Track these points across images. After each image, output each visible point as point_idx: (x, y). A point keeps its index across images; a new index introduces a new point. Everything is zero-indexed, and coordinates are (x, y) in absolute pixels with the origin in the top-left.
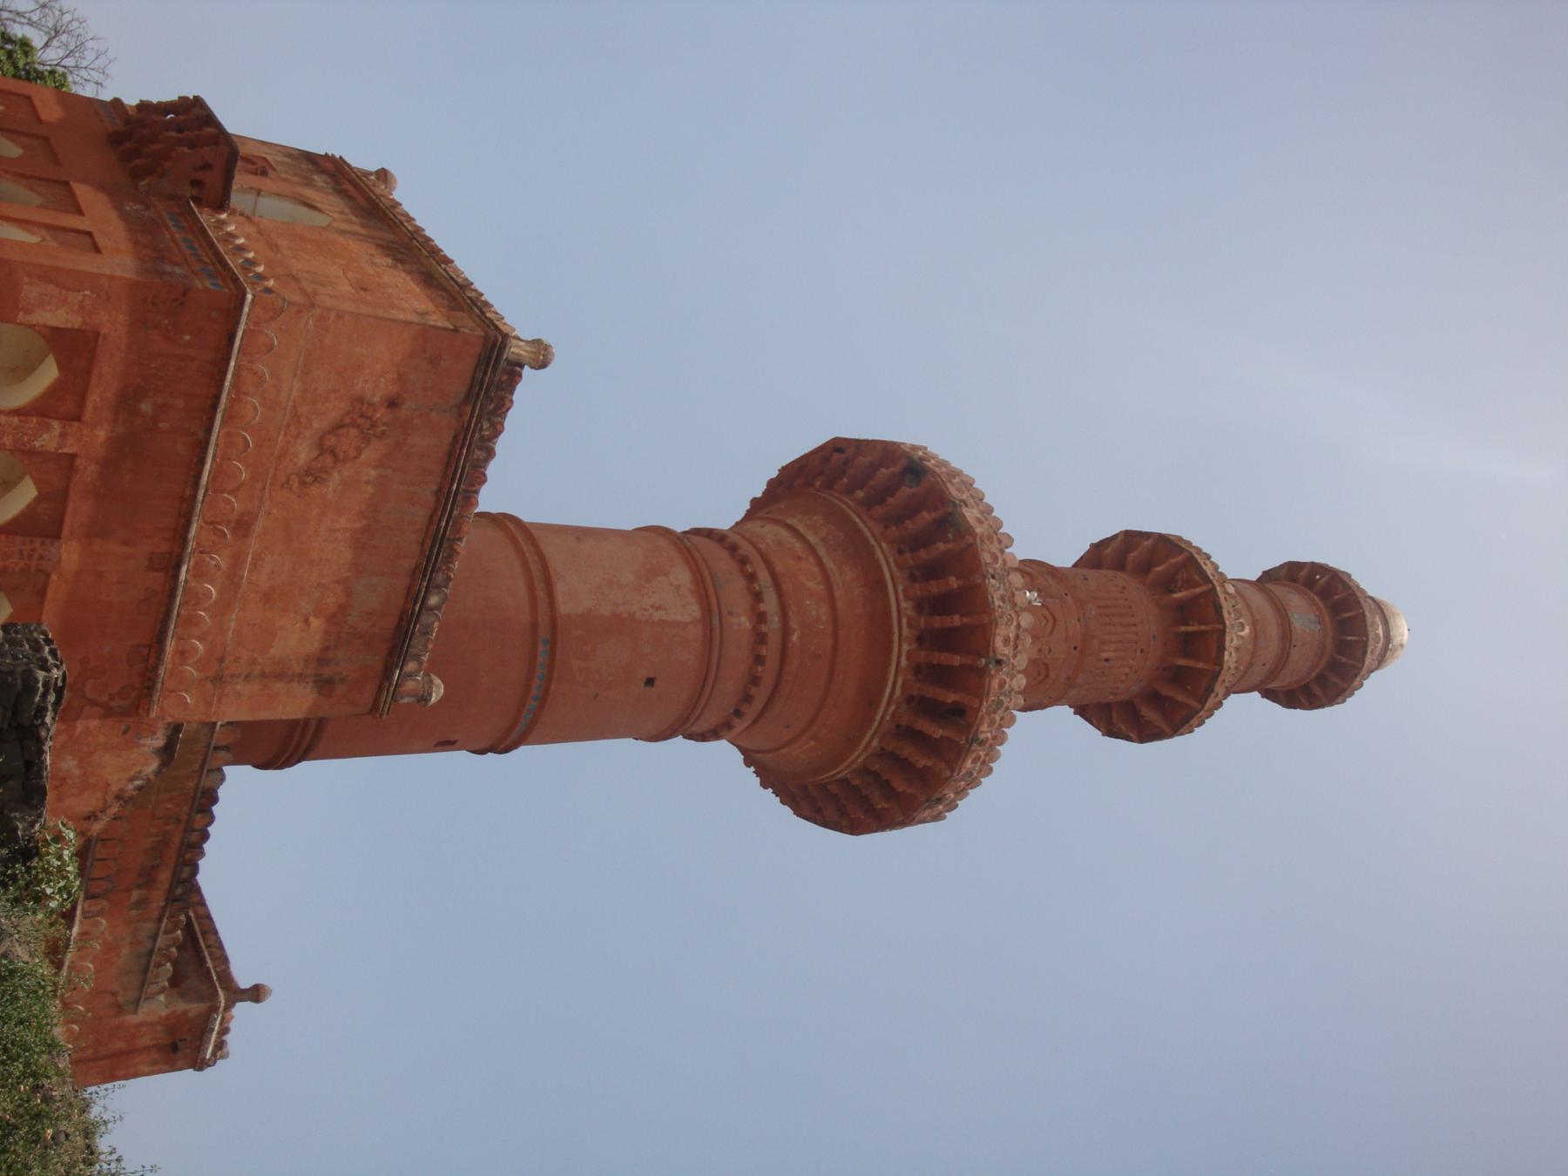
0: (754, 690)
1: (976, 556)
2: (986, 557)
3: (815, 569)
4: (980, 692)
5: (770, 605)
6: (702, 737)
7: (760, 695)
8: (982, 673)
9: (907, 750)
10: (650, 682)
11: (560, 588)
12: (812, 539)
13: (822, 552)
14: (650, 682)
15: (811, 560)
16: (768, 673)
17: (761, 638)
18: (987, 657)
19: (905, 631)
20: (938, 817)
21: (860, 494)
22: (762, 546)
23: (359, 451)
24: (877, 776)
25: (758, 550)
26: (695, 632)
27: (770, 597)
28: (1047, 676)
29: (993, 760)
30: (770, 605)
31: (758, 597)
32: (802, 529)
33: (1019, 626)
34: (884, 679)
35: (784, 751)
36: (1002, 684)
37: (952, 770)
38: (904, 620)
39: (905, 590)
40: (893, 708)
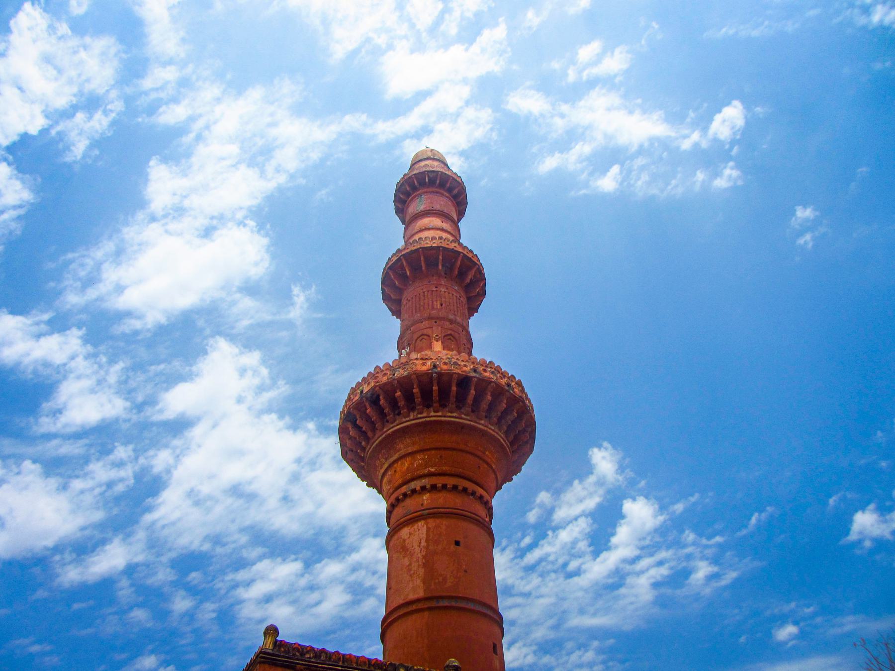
0: (460, 488)
1: (385, 384)
2: (385, 379)
4: (450, 375)
5: (416, 485)
8: (440, 375)
9: (484, 406)
10: (457, 543)
11: (412, 597)
12: (386, 466)
13: (391, 460)
14: (457, 543)
16: (451, 481)
17: (434, 487)
18: (432, 374)
19: (424, 415)
20: (519, 383)
21: (363, 443)
22: (391, 491)
24: (500, 419)
25: (393, 492)
26: (432, 522)
27: (412, 485)
28: (450, 335)
29: (484, 361)
30: (416, 485)
31: (414, 491)
32: (382, 471)
33: (417, 359)
34: (449, 423)
36: (445, 363)
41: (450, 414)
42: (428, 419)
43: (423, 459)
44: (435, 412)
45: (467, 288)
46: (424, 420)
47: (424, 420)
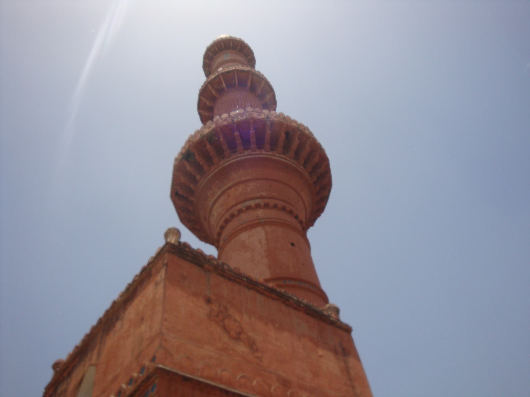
2: (225, 123)
3: (233, 189)
5: (252, 203)
7: (289, 207)
8: (272, 123)
10: (293, 244)
12: (219, 193)
13: (225, 187)
14: (293, 244)
15: (229, 191)
23: (235, 321)
26: (268, 228)
27: (247, 203)
31: (249, 208)
32: (215, 198)
33: (252, 111)
38: (253, 153)
40: (288, 159)
42: (261, 156)
44: (266, 151)
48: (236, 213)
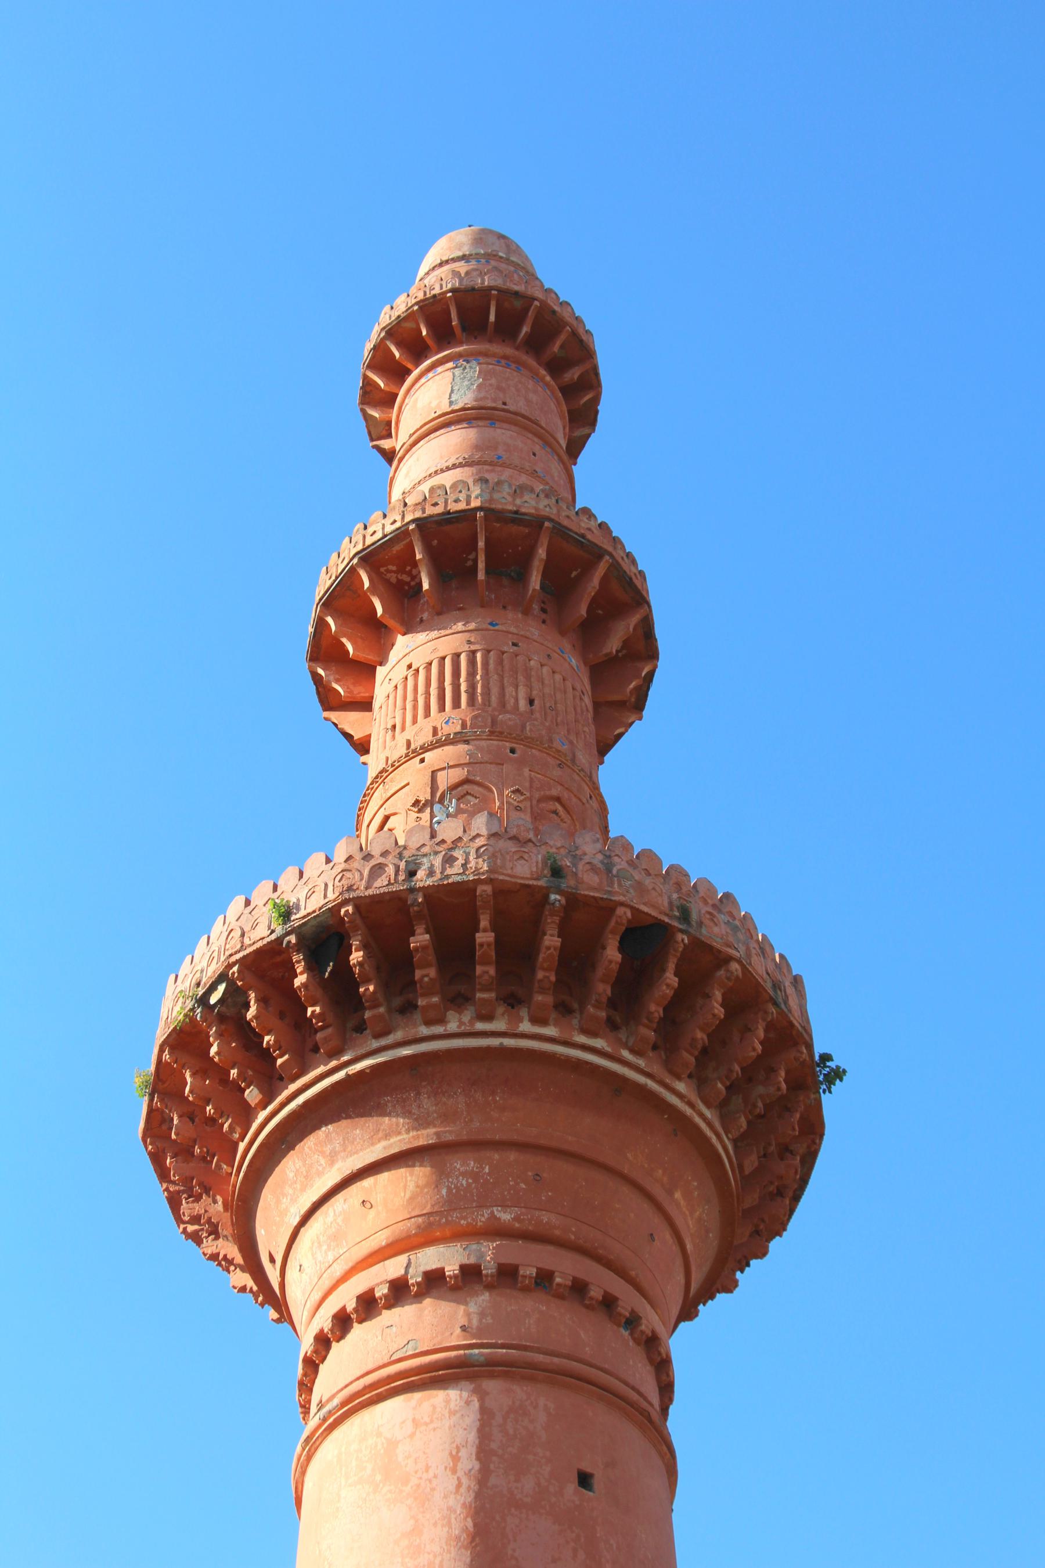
0: (595, 1293)
1: (377, 900)
4: (606, 909)
6: (666, 1390)
7: (602, 1281)
8: (574, 901)
14: (584, 1480)
16: (567, 1267)
19: (499, 1025)
22: (338, 1270)
28: (558, 799)
29: (712, 889)
34: (579, 1065)
35: (689, 1247)
36: (593, 869)
37: (729, 959)
38: (480, 1026)
39: (428, 1023)
40: (626, 1054)
41: (582, 1039)
42: (509, 1042)
43: (475, 1176)
44: (535, 1020)
45: (601, 671)
46: (494, 1042)
47: (494, 1042)
48: (382, 1291)
